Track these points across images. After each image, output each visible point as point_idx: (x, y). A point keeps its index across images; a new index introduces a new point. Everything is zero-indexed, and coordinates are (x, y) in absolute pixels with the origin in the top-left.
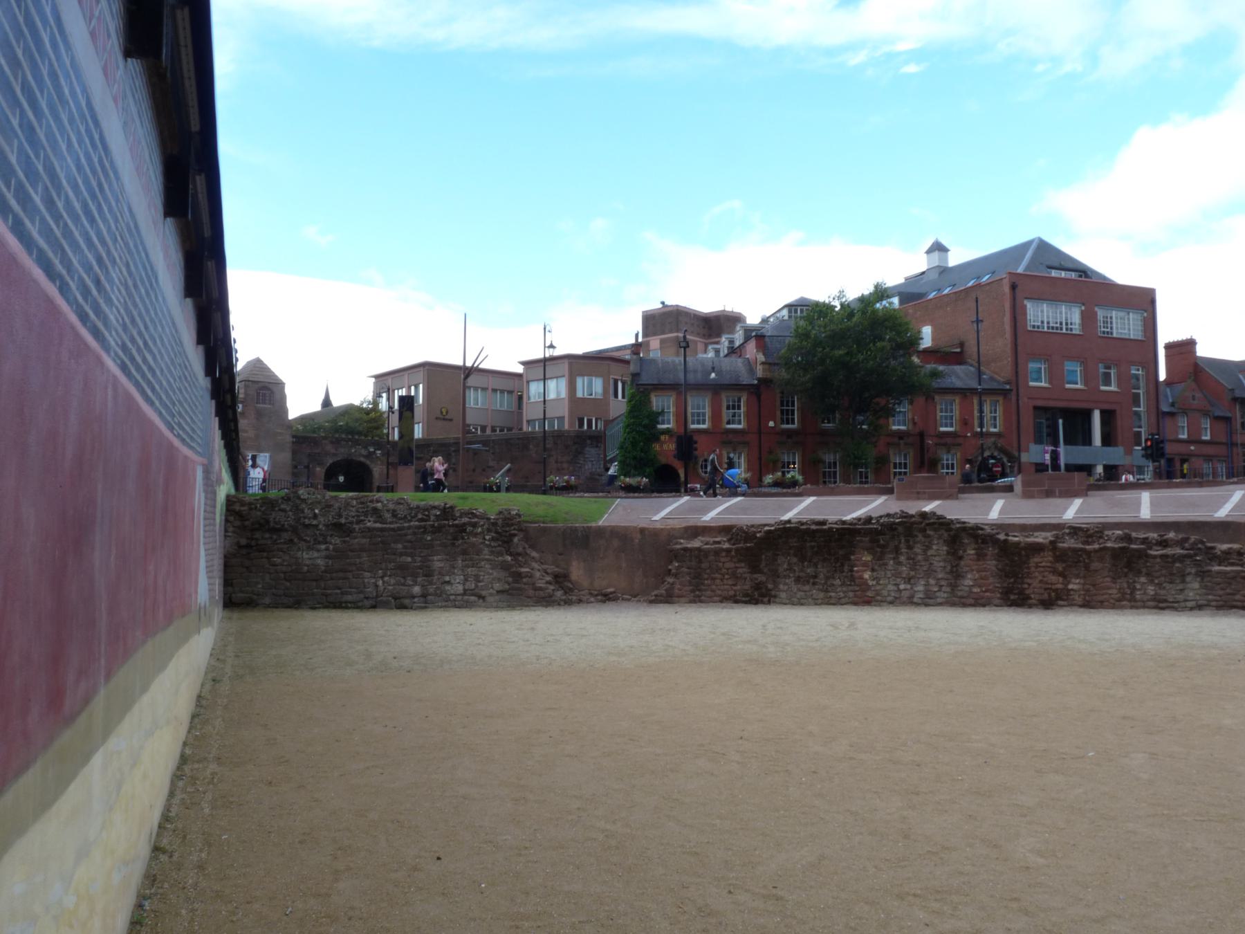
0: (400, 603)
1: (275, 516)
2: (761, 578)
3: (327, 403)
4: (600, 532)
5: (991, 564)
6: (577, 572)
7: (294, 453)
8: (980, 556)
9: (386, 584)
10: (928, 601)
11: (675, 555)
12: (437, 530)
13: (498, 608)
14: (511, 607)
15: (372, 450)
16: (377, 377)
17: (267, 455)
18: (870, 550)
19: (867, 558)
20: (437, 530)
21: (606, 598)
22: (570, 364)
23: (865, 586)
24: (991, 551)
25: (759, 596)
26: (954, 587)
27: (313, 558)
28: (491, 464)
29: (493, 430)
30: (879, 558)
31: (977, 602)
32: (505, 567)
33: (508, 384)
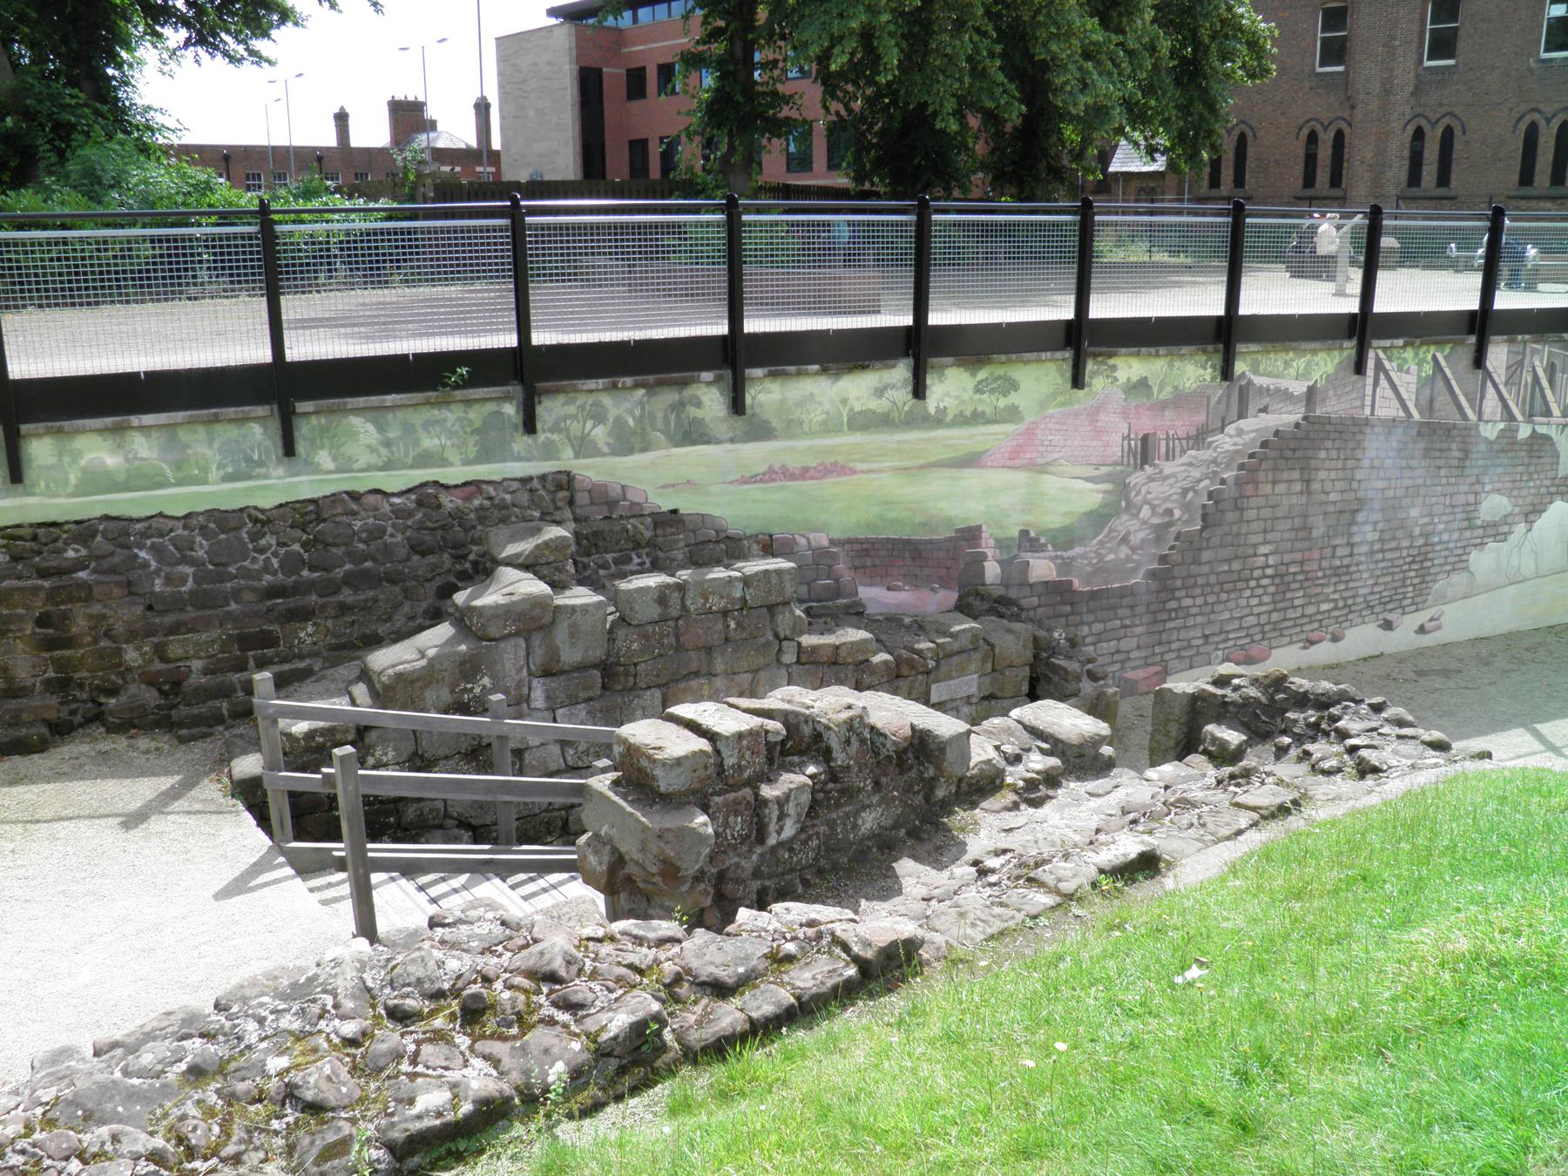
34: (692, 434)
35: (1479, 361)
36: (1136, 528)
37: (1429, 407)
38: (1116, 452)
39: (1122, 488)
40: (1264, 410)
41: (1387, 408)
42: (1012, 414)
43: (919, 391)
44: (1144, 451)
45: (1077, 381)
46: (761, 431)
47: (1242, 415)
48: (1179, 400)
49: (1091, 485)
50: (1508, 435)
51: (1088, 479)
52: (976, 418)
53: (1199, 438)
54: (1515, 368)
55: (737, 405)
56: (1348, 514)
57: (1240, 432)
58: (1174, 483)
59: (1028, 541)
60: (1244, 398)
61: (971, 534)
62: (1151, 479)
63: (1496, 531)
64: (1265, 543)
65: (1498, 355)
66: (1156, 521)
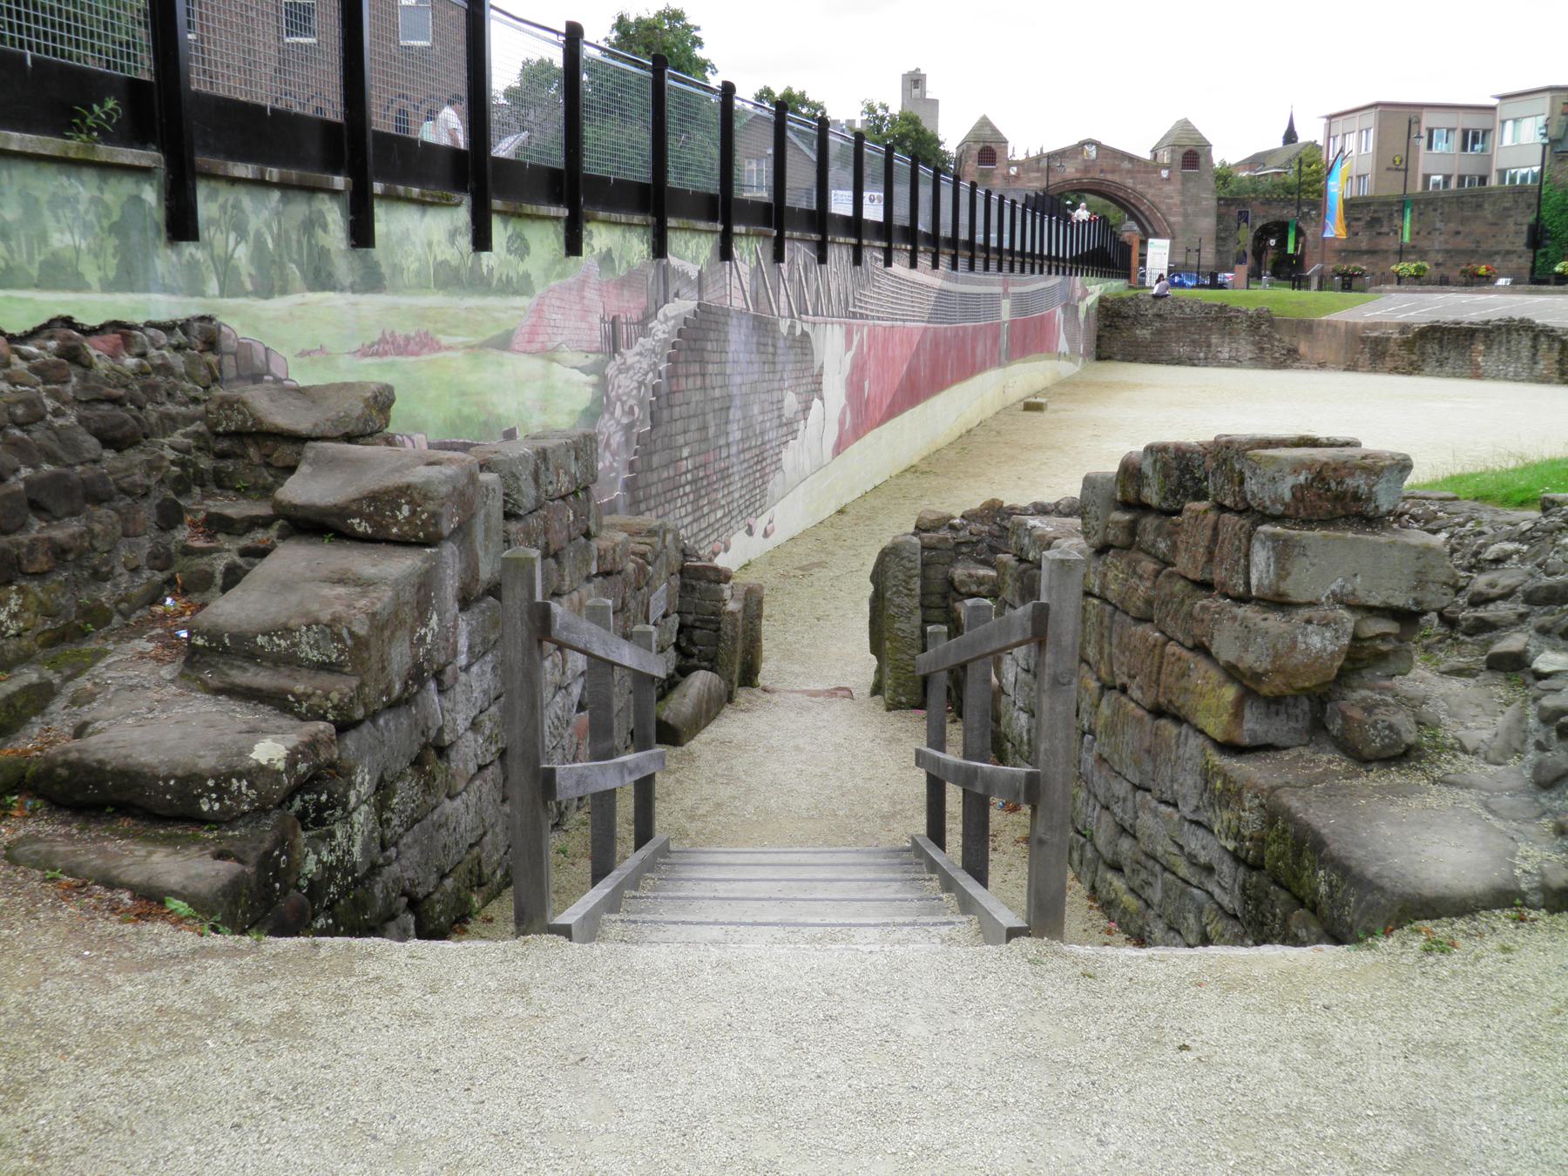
0: (1191, 362)
1: (1124, 310)
2: (1414, 358)
3: (1290, 136)
4: (1320, 323)
5: (1556, 355)
6: (1303, 348)
7: (1220, 218)
8: (1550, 349)
9: (1184, 350)
10: (1516, 378)
11: (1363, 340)
12: (1216, 319)
13: (1248, 367)
14: (1256, 367)
15: (1306, 210)
16: (1330, 117)
17: (1166, 243)
18: (1484, 342)
19: (1482, 348)
20: (1216, 319)
21: (1322, 366)
22: (1553, 99)
23: (1478, 367)
24: (1557, 346)
25: (1413, 369)
26: (1532, 369)
27: (1143, 333)
28: (1438, 225)
29: (1461, 179)
30: (1489, 347)
31: (1544, 380)
32: (1254, 343)
33: (1473, 122)
34: (320, 279)
38: (597, 335)
39: (603, 384)
40: (677, 295)
41: (738, 303)
43: (481, 241)
44: (614, 342)
45: (573, 246)
46: (372, 281)
47: (666, 302)
49: (583, 377)
51: (582, 369)
53: (644, 323)
55: (361, 234)
57: (667, 319)
62: (620, 371)
64: (686, 444)
66: (625, 421)
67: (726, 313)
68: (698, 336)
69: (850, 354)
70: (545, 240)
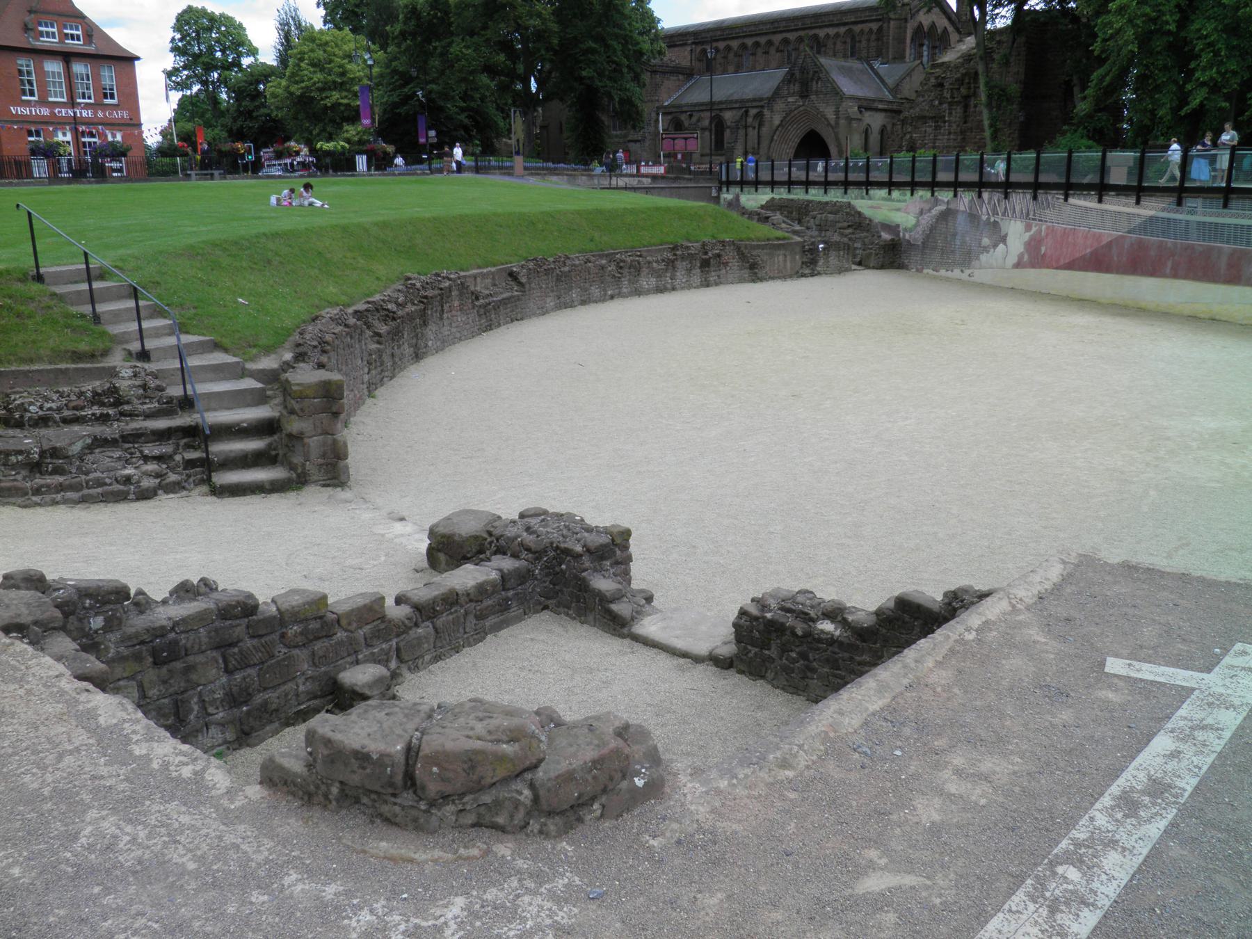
34: (863, 198)
35: (980, 196)
36: (920, 229)
37: (971, 208)
41: (962, 208)
42: (905, 201)
44: (921, 213)
46: (870, 199)
48: (926, 201)
50: (989, 219)
52: (899, 201)
53: (930, 210)
54: (990, 199)
56: (954, 235)
58: (927, 219)
59: (905, 230)
60: (937, 202)
61: (898, 226)
63: (986, 249)
65: (985, 195)
67: (957, 211)
68: (947, 215)
69: (1028, 235)
70: (909, 193)
